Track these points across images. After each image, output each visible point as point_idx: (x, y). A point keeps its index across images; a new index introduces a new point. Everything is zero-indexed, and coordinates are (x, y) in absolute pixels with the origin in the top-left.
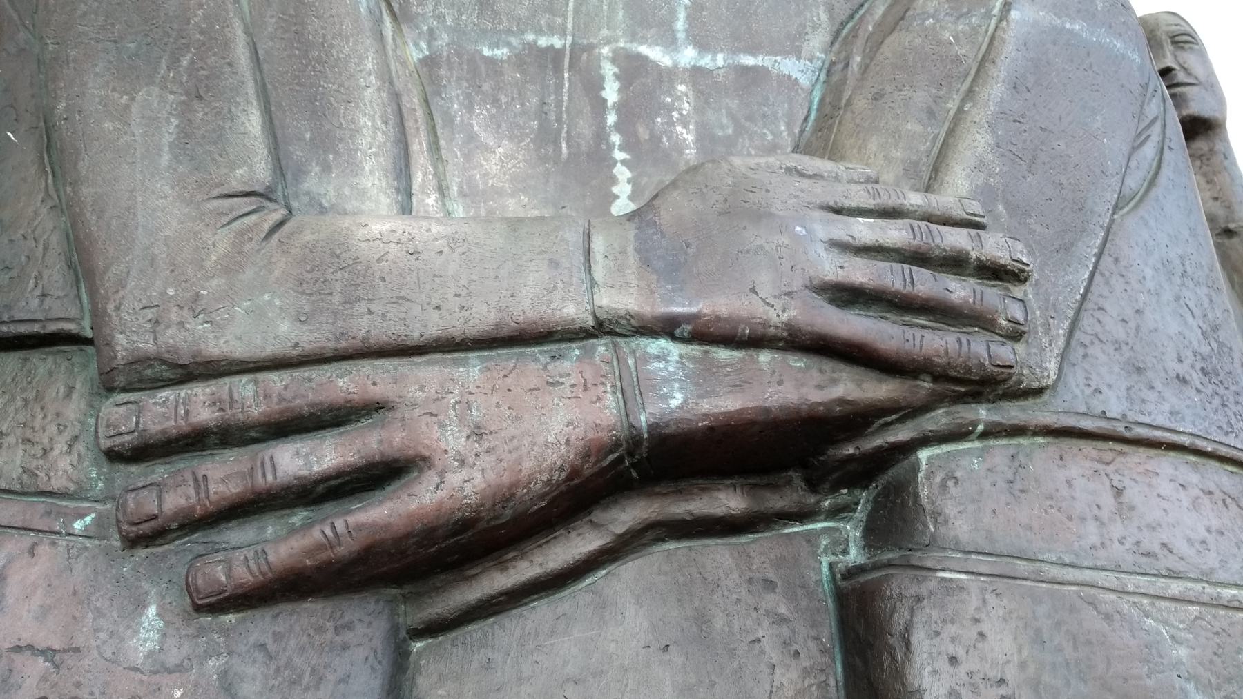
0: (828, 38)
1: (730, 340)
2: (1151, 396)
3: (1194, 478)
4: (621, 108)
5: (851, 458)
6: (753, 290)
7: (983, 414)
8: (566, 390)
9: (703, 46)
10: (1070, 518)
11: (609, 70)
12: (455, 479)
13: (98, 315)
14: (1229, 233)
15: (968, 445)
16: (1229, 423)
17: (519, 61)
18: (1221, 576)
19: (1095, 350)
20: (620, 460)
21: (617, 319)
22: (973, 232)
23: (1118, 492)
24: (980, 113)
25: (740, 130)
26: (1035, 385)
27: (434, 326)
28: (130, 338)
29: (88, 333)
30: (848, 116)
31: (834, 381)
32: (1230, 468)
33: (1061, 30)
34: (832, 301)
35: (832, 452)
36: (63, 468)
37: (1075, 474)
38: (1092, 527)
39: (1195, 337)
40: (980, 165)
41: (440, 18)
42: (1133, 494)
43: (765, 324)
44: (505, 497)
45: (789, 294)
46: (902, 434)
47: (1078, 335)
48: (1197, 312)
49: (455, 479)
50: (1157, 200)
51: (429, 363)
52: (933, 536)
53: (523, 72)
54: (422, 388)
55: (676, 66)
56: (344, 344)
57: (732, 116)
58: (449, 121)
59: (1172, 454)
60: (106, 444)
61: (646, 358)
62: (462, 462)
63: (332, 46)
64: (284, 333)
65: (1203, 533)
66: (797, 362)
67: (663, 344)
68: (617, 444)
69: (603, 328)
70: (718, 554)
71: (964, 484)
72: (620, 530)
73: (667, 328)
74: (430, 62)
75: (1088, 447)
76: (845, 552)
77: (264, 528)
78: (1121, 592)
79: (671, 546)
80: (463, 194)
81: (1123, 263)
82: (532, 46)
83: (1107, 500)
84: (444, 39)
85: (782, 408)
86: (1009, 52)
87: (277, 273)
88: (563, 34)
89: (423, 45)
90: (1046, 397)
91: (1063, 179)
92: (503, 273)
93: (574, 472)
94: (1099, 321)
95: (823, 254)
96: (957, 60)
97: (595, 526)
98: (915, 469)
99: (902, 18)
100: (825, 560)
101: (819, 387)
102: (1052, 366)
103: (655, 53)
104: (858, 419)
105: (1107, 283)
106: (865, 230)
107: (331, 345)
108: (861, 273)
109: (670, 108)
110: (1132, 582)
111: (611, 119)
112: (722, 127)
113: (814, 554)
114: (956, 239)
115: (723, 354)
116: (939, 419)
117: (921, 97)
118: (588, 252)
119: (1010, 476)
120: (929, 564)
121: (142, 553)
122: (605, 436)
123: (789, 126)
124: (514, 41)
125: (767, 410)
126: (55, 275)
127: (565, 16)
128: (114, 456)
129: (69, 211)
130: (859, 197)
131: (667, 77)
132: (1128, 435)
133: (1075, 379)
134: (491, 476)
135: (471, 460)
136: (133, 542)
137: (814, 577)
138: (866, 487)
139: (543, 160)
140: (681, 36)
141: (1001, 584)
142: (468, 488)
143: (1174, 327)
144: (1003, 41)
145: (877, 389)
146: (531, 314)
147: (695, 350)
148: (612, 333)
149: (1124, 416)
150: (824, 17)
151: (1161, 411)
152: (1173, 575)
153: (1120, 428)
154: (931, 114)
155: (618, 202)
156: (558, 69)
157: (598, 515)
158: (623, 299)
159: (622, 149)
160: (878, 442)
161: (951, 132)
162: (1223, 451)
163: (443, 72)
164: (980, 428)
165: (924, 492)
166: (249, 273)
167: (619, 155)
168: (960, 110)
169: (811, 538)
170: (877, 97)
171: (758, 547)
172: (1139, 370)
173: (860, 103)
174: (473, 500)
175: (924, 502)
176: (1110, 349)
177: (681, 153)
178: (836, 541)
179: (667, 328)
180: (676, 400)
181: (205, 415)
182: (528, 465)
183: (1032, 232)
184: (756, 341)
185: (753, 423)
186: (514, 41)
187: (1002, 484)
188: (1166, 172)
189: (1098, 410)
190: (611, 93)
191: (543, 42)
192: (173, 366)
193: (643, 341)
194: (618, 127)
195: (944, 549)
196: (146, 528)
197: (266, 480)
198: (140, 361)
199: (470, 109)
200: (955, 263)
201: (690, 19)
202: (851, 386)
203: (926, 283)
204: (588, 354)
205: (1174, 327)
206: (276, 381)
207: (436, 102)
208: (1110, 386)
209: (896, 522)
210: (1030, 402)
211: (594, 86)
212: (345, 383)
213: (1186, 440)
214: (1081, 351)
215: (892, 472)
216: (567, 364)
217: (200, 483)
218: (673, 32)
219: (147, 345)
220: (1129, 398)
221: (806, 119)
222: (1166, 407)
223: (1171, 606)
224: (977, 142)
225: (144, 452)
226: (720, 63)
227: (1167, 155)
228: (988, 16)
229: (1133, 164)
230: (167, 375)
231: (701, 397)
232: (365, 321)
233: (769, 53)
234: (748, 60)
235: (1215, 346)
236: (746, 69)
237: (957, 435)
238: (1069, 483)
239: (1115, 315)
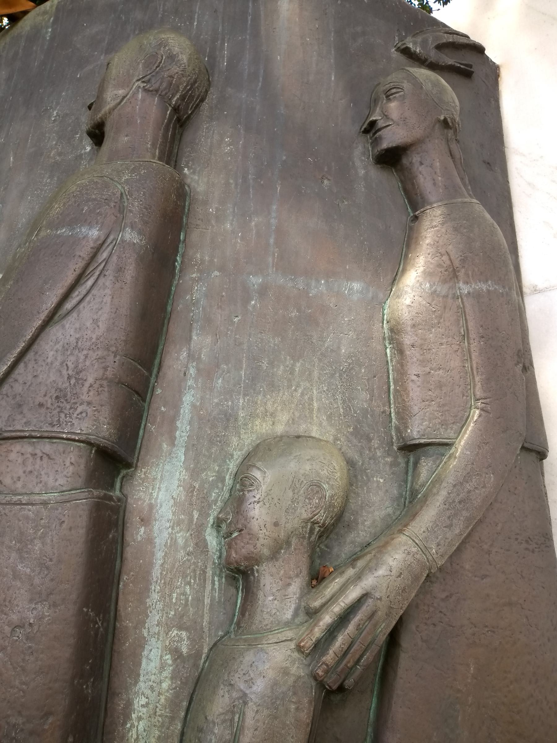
32: (55, 441)
94: (12, 387)
105: (26, 366)
205: (53, 377)
235: (73, 381)
239: (21, 382)
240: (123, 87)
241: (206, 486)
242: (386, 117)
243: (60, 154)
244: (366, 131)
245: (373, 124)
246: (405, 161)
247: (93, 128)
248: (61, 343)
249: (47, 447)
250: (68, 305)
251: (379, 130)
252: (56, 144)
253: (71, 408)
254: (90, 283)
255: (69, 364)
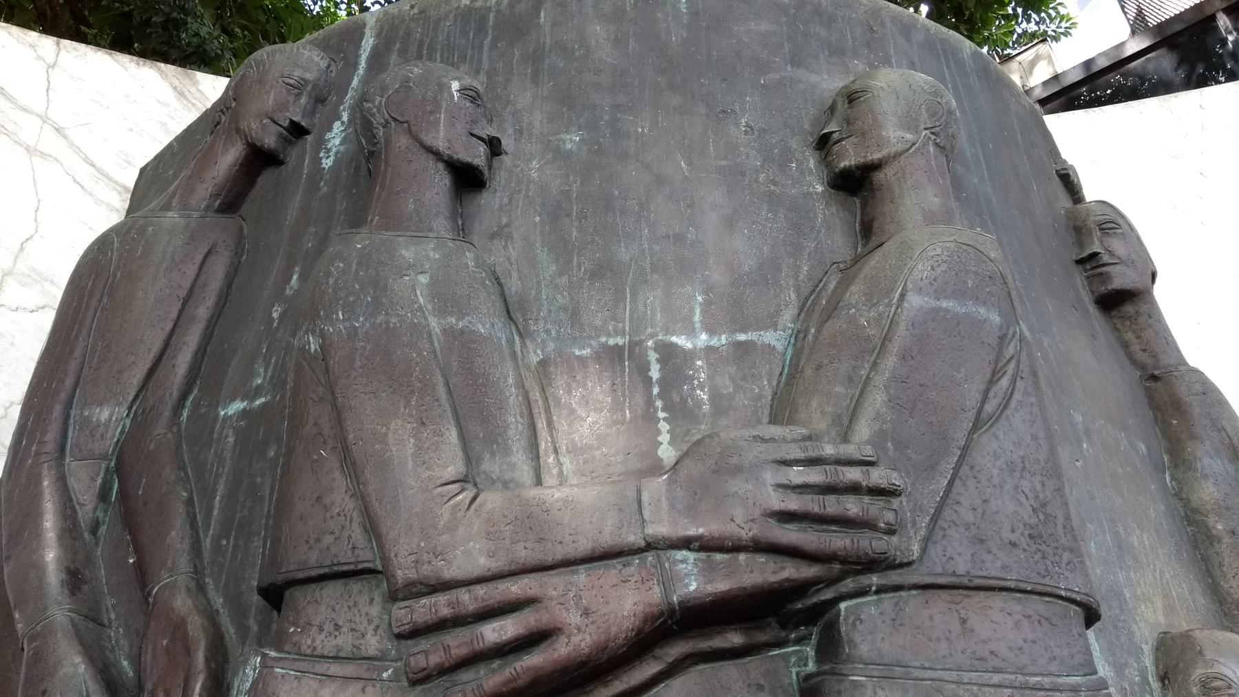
0: (796, 312)
1: (722, 549)
2: (989, 558)
3: (1018, 608)
4: (661, 382)
5: (800, 610)
6: (732, 520)
7: (875, 580)
8: (632, 585)
9: (712, 332)
10: (930, 640)
11: (653, 356)
12: (576, 639)
13: (385, 559)
14: (1154, 378)
15: (869, 598)
16: (1046, 570)
17: (598, 357)
18: (1031, 669)
19: (952, 532)
20: (665, 622)
21: (657, 541)
22: (864, 468)
23: (964, 621)
24: (879, 379)
25: (737, 387)
26: (905, 560)
27: (559, 553)
28: (403, 573)
29: (380, 568)
30: (801, 381)
31: (783, 568)
32: (1047, 599)
33: (937, 310)
34: (779, 521)
35: (789, 607)
36: (372, 644)
37: (935, 613)
38: (944, 644)
39: (1026, 513)
40: (878, 416)
41: (548, 332)
42: (974, 622)
43: (740, 539)
44: (602, 648)
45: (752, 520)
46: (828, 594)
47: (940, 522)
48: (1031, 495)
49: (576, 639)
50: (1007, 417)
51: (558, 574)
52: (848, 655)
53: (600, 364)
54: (555, 589)
55: (695, 348)
56: (513, 567)
57: (732, 379)
58: (558, 403)
59: (1004, 593)
60: (396, 630)
61: (675, 562)
62: (579, 630)
63: (489, 374)
64: (482, 564)
65: (1021, 643)
66: (761, 559)
67: (685, 552)
68: (662, 614)
69: (651, 546)
70: (730, 670)
71: (868, 623)
72: (670, 660)
73: (686, 543)
74: (544, 363)
75: (944, 594)
76: (806, 665)
77: (478, 672)
78: (959, 683)
79: (701, 667)
80: (569, 452)
81: (977, 468)
82: (605, 345)
83: (956, 626)
84: (551, 346)
85: (753, 587)
86: (902, 330)
87: (476, 528)
88: (623, 334)
89: (539, 352)
90: (914, 566)
91: (933, 419)
92: (594, 519)
93: (640, 631)
95: (772, 493)
96: (868, 339)
97: (656, 658)
98: (839, 614)
99: (836, 309)
100: (794, 670)
101: (774, 572)
102: (916, 548)
103: (681, 341)
104: (800, 588)
105: (964, 484)
106: (797, 475)
107: (506, 568)
108: (793, 503)
109: (692, 378)
110: (966, 677)
111: (656, 390)
112: (726, 387)
113: (788, 667)
114: (853, 474)
115: (719, 557)
116: (849, 584)
117: (844, 367)
118: (640, 502)
119: (893, 616)
120: (844, 672)
121: (419, 688)
122: (655, 610)
123: (769, 381)
124: (593, 343)
125: (745, 589)
126: (358, 535)
127: (624, 322)
128: (400, 637)
129: (361, 497)
130: (796, 453)
131: (689, 356)
132: (970, 584)
133: (935, 552)
134: (595, 637)
135: (583, 628)
136: (414, 683)
137: (787, 681)
138: (815, 625)
139: (615, 423)
140: (698, 326)
141: (884, 683)
142: (583, 644)
143: (1011, 507)
144: (898, 323)
145: (809, 571)
146: (610, 543)
147: (703, 555)
148: (657, 549)
149: (968, 573)
150: (793, 296)
151: (992, 567)
152: (996, 670)
153: (965, 581)
154: (850, 379)
155: (662, 447)
156: (621, 360)
157: (658, 652)
158: (660, 528)
159: (663, 410)
160: (815, 600)
161: (862, 393)
162: (1039, 588)
163: (552, 369)
164: (874, 588)
165: (843, 629)
166: (461, 530)
167: (661, 415)
168: (868, 377)
169: (785, 657)
170: (819, 368)
171: (753, 664)
172: (982, 541)
173: (809, 372)
174: (587, 651)
175: (843, 634)
176: (962, 529)
177: (700, 408)
178: (799, 658)
179: (686, 543)
180: (692, 588)
181: (445, 612)
182: (614, 629)
183: (909, 459)
184: (737, 548)
185: (737, 596)
186: (593, 343)
187: (888, 622)
188: (1017, 396)
189: (951, 571)
190: (655, 373)
191: (611, 342)
192: (427, 585)
193: (673, 552)
194: (660, 396)
195: (853, 662)
196: (421, 675)
197: (479, 646)
198: (411, 584)
199: (569, 392)
200: (854, 489)
201: (703, 312)
202: (793, 570)
203: (832, 506)
204: (643, 560)
205: (1011, 507)
206: (481, 590)
207: (549, 390)
208: (959, 554)
209: (831, 647)
210: (904, 570)
211: (643, 369)
212: (515, 588)
213: (1012, 585)
214: (941, 533)
215: (827, 616)
216: (632, 568)
217: (447, 649)
218: (693, 323)
219: (413, 575)
220: (973, 561)
221: (781, 374)
222: (999, 564)
223: (992, 690)
224: (877, 400)
225: (416, 633)
226: (724, 342)
227: (1019, 383)
228: (889, 305)
229: (991, 394)
230: (424, 590)
231: (706, 583)
232: (523, 553)
233: (755, 330)
234: (742, 337)
235: (1042, 517)
236: (740, 343)
237: (861, 593)
238: (931, 618)
240: (909, 130)
241: (1136, 688)
242: (1111, 253)
243: (774, 183)
244: (1080, 262)
245: (1095, 255)
246: (1128, 309)
247: (858, 167)
248: (1002, 459)
249: (1037, 605)
250: (989, 408)
251: (1104, 265)
252: (762, 166)
253: (1055, 554)
254: (1005, 382)
255: (1027, 491)
